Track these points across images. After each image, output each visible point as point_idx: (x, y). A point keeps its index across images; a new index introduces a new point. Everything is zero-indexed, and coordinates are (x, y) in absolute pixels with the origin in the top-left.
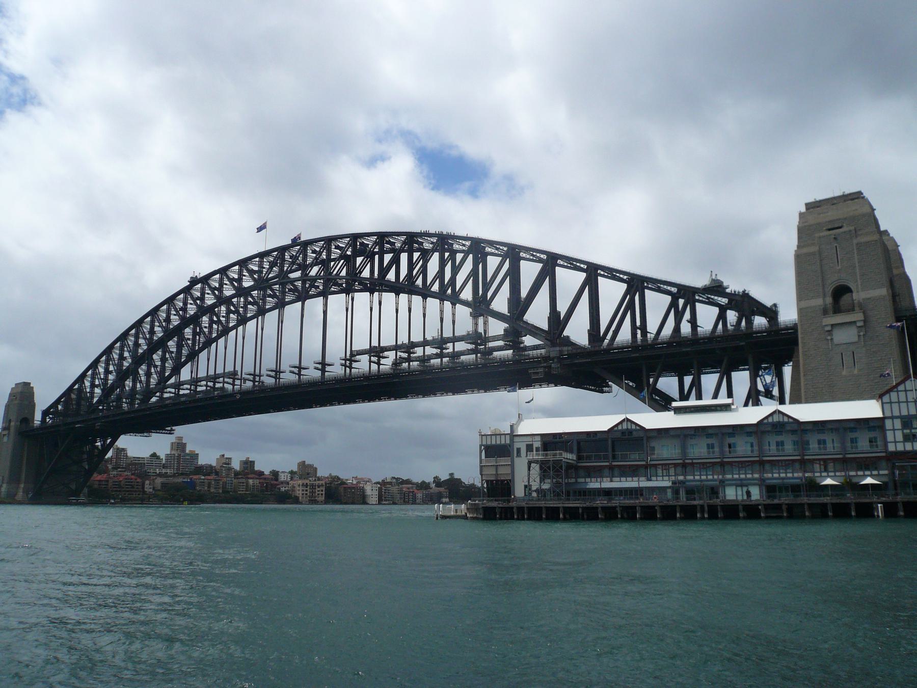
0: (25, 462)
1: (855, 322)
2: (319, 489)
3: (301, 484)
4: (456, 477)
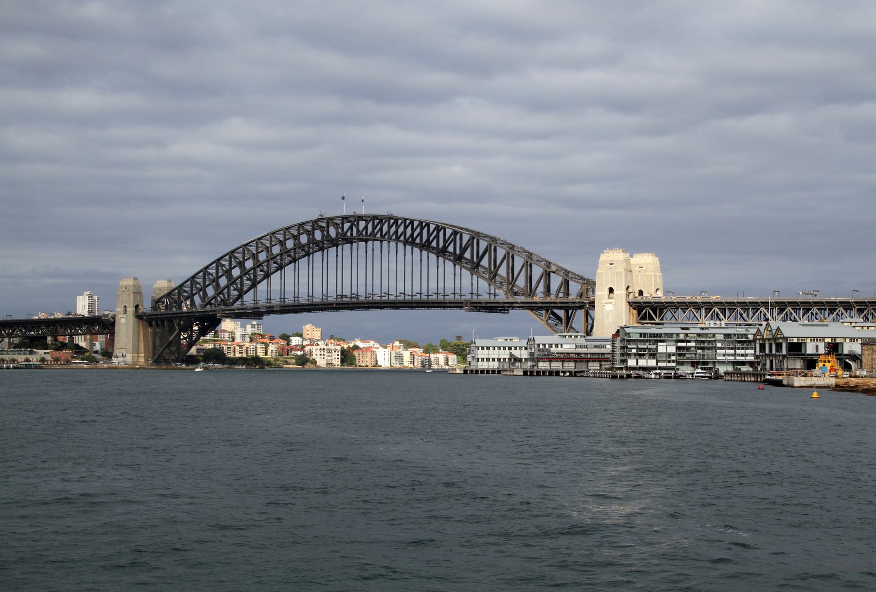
0: (142, 337)
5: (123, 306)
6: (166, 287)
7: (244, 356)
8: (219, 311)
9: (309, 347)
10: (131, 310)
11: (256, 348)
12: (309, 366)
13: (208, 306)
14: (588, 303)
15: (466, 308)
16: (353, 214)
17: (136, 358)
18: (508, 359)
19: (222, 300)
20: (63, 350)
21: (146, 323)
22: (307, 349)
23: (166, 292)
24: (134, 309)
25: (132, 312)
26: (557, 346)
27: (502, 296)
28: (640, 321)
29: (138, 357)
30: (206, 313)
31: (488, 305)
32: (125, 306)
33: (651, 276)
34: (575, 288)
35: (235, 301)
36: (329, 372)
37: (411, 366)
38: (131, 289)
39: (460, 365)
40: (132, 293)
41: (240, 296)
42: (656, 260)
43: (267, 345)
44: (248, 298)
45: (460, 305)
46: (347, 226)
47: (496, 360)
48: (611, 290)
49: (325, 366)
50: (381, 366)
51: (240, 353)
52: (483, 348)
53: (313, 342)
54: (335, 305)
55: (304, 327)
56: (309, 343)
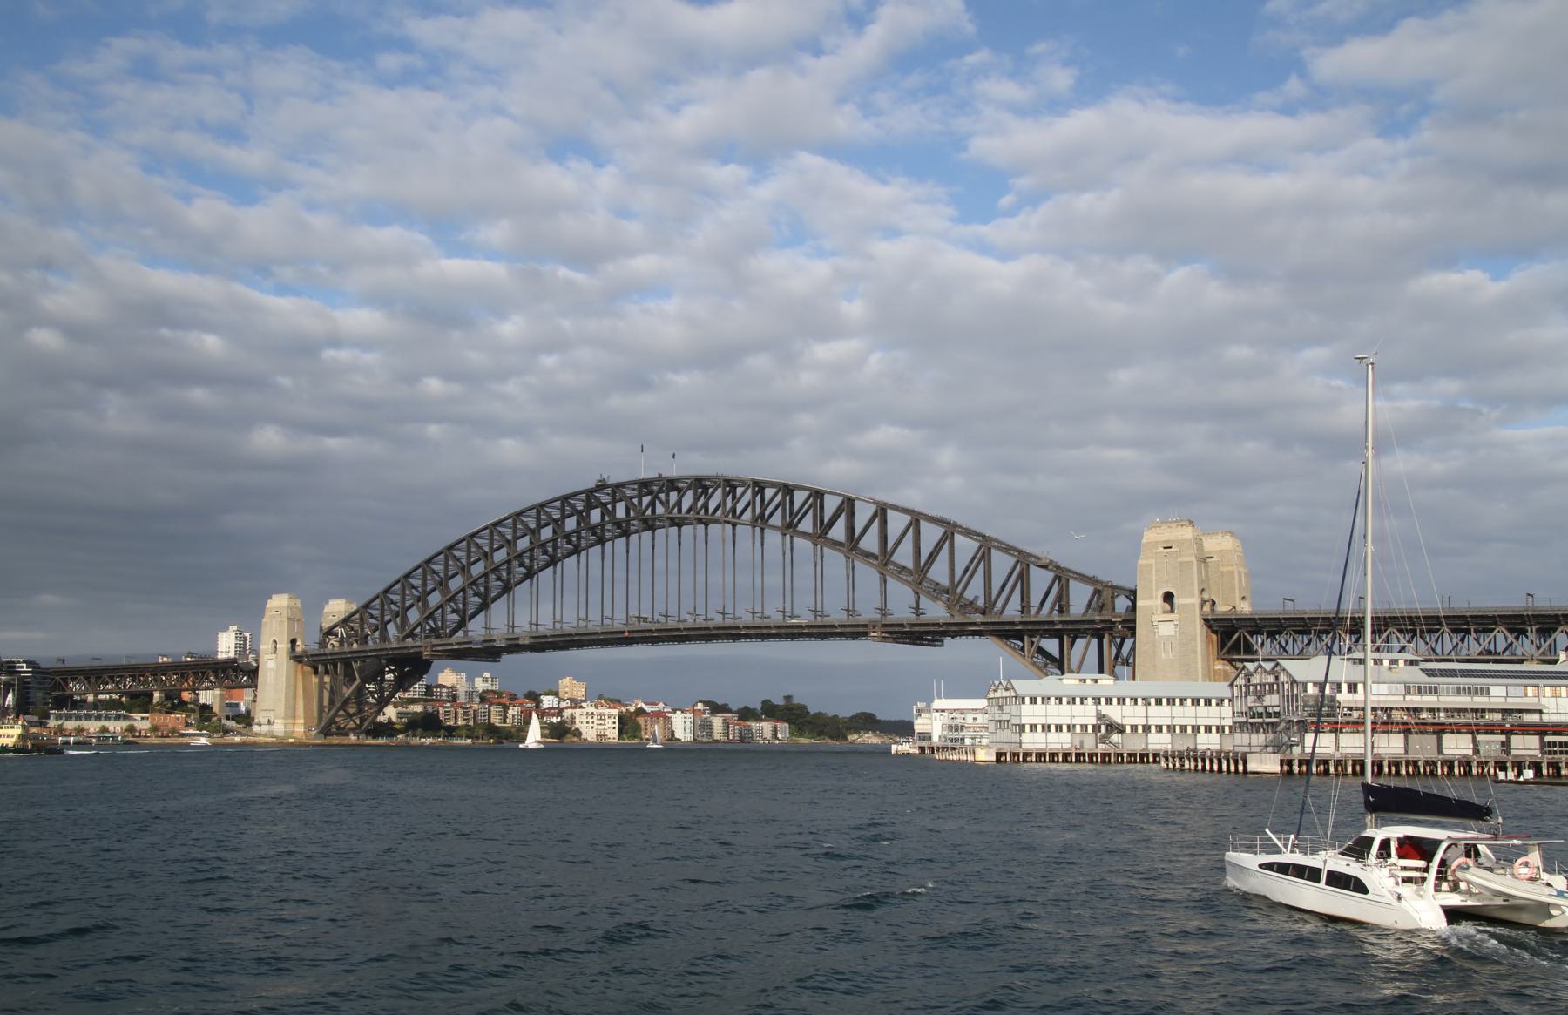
4: (795, 701)
5: (271, 642)
6: (343, 610)
7: (471, 723)
8: (426, 647)
9: (570, 711)
10: (284, 646)
11: (489, 712)
12: (568, 739)
13: (410, 640)
14: (1120, 623)
15: (873, 634)
17: (291, 726)
18: (1094, 726)
19: (432, 630)
20: (171, 713)
21: (309, 669)
22: (567, 713)
23: (342, 616)
24: (289, 645)
25: (285, 650)
26: (1353, 688)
27: (936, 611)
28: (1227, 656)
29: (294, 724)
30: (406, 651)
31: (916, 629)
32: (275, 642)
33: (1233, 572)
34: (1079, 597)
35: (455, 631)
36: (600, 751)
37: (724, 739)
38: (285, 614)
39: (794, 738)
40: (285, 619)
41: (461, 624)
42: (1238, 543)
43: (506, 708)
44: (476, 629)
45: (861, 630)
46: (646, 500)
47: (1214, 729)
48: (1168, 597)
49: (595, 740)
50: (679, 740)
51: (464, 719)
52: (1033, 701)
53: (575, 703)
54: (627, 634)
55: (560, 681)
56: (569, 705)
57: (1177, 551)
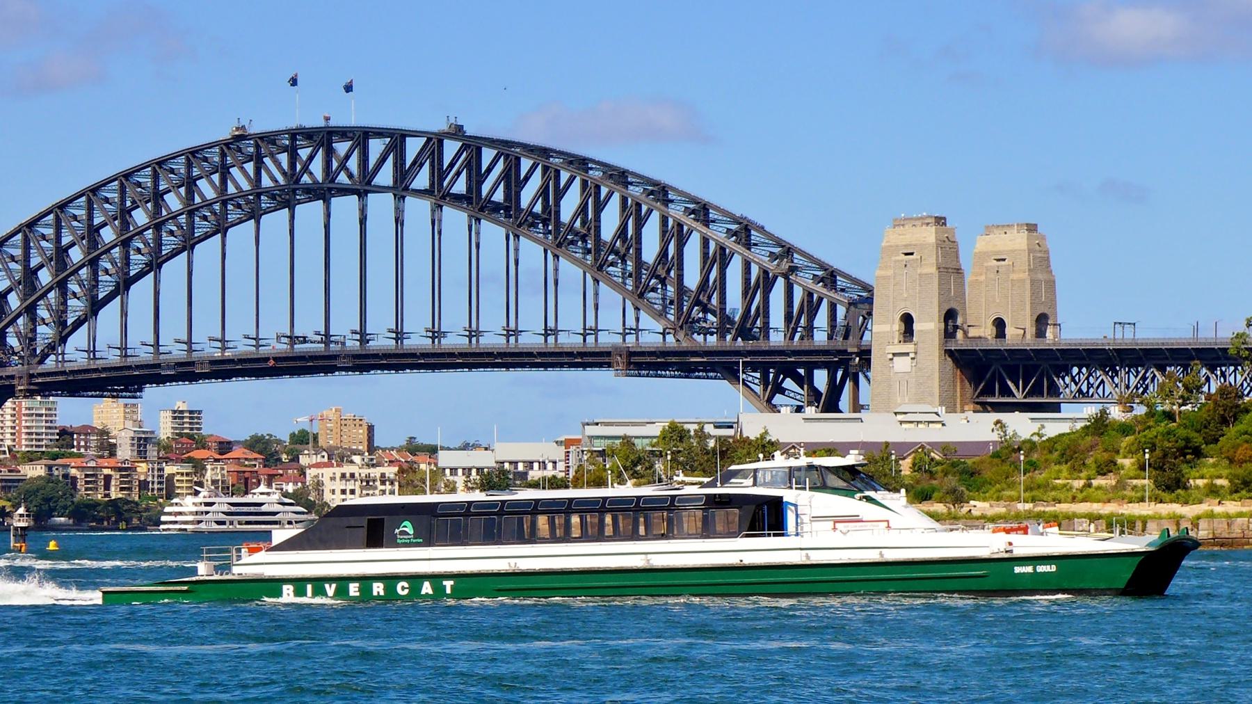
1: (907, 354)
2: (383, 487)
3: (338, 476)
16: (322, 123)
26: (543, 465)
54: (271, 363)
56: (326, 459)
57: (917, 259)
